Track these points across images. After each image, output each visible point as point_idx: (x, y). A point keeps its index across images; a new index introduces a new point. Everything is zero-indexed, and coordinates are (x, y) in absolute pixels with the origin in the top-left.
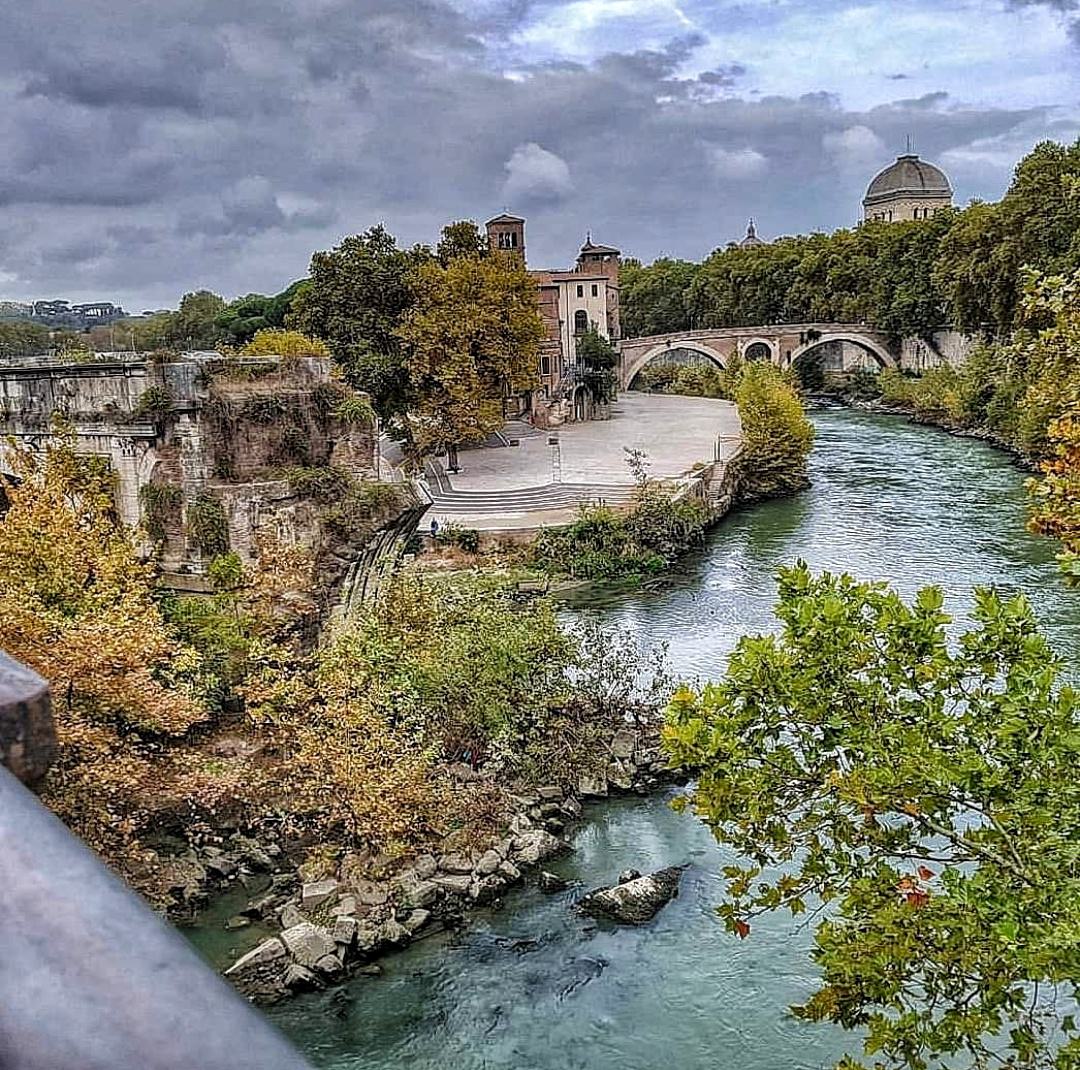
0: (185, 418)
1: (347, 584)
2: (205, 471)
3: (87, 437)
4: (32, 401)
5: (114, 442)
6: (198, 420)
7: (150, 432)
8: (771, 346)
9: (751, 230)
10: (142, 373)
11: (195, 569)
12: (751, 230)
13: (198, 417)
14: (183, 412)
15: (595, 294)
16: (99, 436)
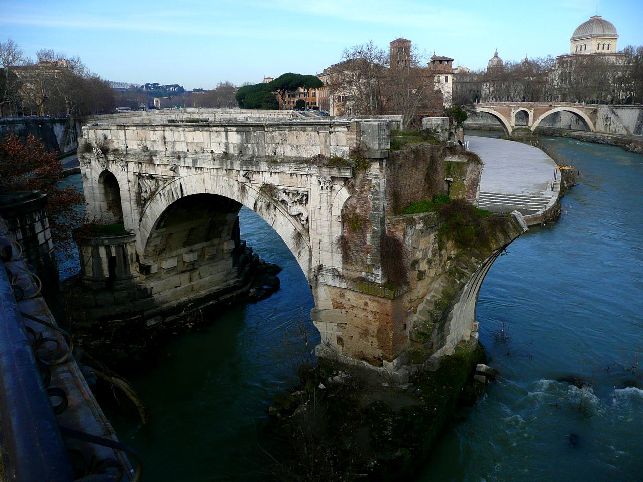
0: (376, 166)
1: (466, 288)
2: (386, 205)
3: (291, 175)
4: (247, 147)
5: (314, 180)
6: (384, 164)
7: (347, 174)
8: (529, 112)
9: (496, 53)
10: (344, 129)
11: (375, 278)
12: (496, 53)
13: (384, 164)
14: (376, 160)
15: (446, 81)
16: (301, 175)
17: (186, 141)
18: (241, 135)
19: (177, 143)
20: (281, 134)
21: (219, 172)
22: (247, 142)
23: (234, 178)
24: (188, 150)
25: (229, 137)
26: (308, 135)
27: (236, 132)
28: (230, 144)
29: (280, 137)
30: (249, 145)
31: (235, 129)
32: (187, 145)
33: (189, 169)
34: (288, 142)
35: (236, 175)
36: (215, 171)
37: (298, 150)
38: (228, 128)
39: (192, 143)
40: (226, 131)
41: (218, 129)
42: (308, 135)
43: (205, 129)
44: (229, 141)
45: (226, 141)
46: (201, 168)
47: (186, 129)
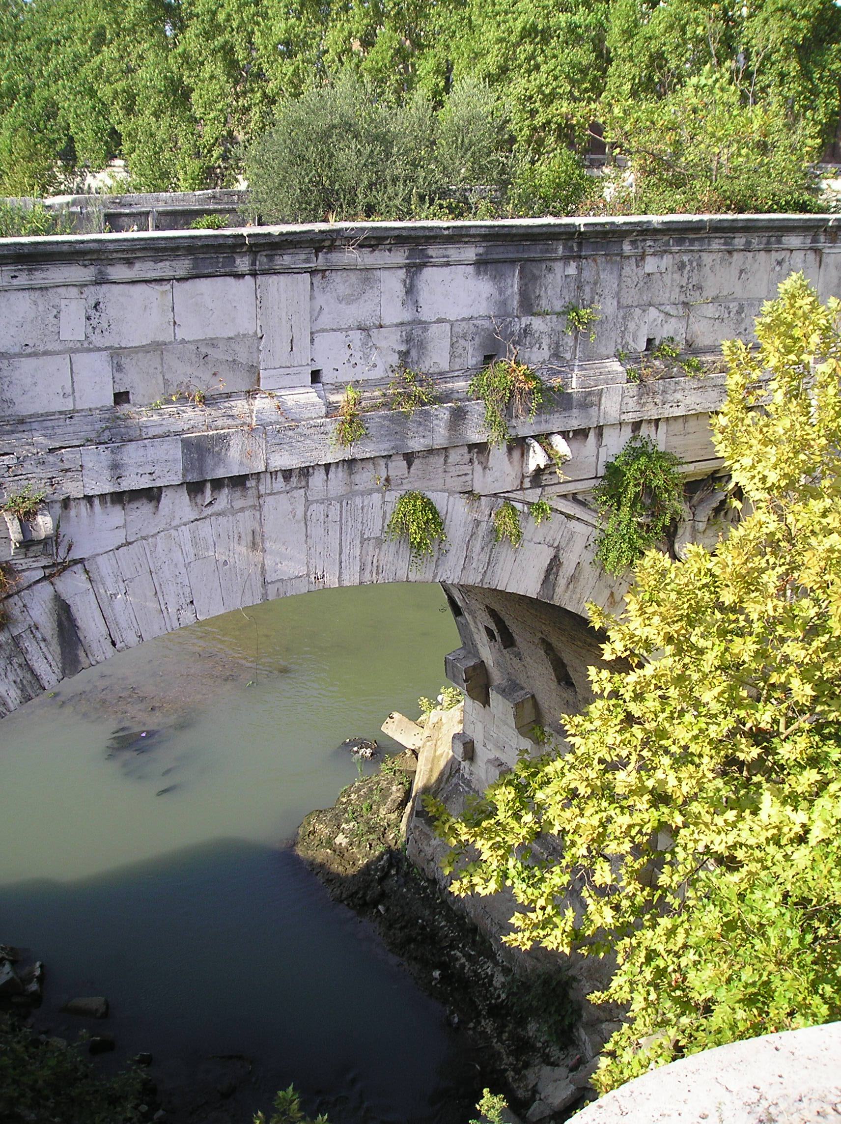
4: (526, 331)
17: (97, 340)
18: (497, 277)
19: (27, 365)
20: (681, 267)
21: (357, 478)
22: (528, 306)
23: (457, 484)
24: (121, 398)
25: (424, 295)
26: (779, 263)
27: (470, 269)
28: (434, 329)
29: (677, 276)
30: (538, 324)
31: (470, 253)
32: (119, 368)
33: (145, 508)
34: (705, 294)
35: (467, 469)
36: (338, 476)
37: (740, 322)
38: (432, 251)
39: (157, 347)
40: (414, 268)
41: (367, 258)
42: (779, 263)
43: (286, 260)
44: (426, 314)
45: (407, 316)
46: (239, 482)
47: (118, 272)
